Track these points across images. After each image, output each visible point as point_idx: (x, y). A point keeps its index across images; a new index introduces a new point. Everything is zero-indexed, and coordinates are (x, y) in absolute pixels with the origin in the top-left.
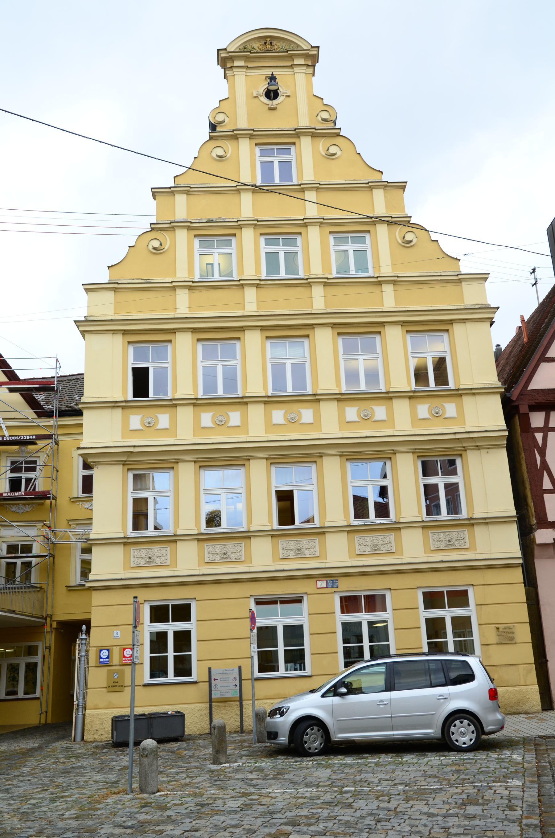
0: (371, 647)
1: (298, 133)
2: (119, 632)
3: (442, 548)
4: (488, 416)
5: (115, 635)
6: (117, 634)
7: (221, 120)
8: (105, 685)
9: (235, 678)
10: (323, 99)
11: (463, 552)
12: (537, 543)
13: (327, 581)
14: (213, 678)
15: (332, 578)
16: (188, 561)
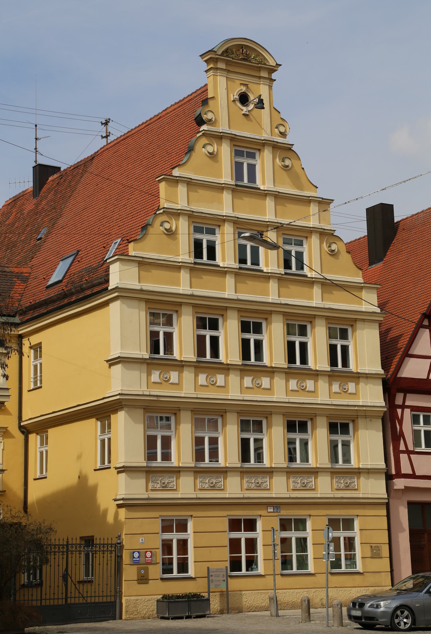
0: (171, 554)
1: (263, 144)
2: (143, 539)
3: (341, 488)
4: (372, 396)
5: (141, 541)
6: (142, 540)
7: (210, 118)
8: (136, 579)
9: (224, 575)
10: (279, 112)
11: (353, 492)
12: (395, 487)
13: (273, 507)
14: (210, 574)
15: (277, 505)
16: (186, 488)
